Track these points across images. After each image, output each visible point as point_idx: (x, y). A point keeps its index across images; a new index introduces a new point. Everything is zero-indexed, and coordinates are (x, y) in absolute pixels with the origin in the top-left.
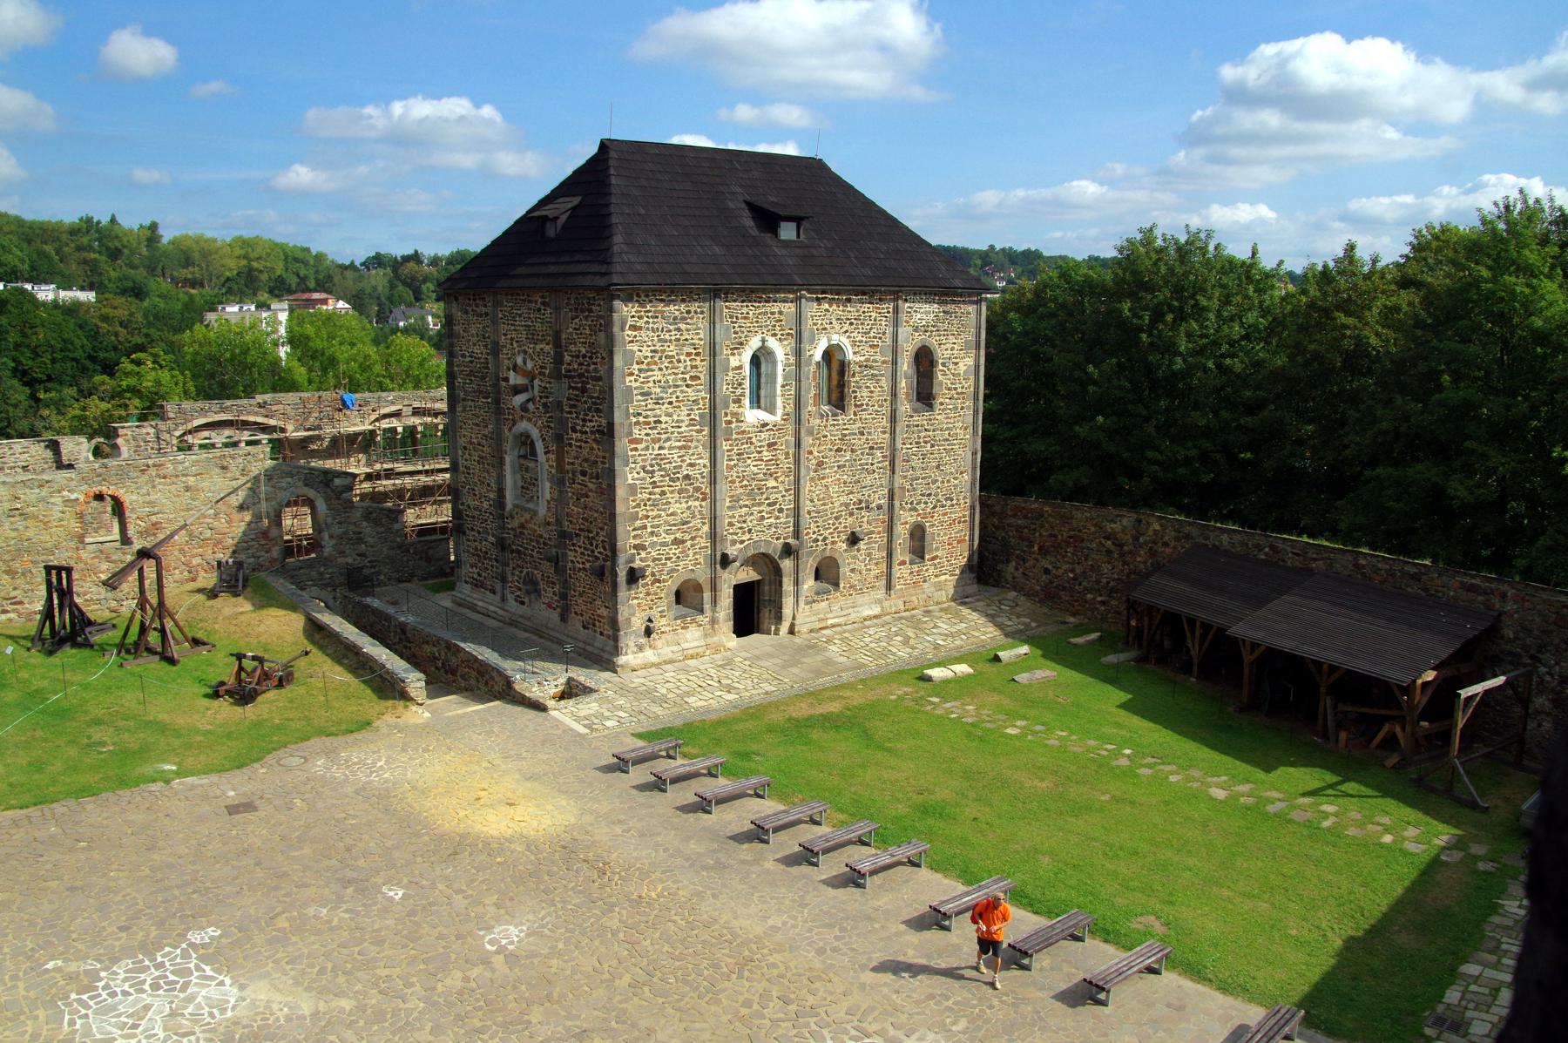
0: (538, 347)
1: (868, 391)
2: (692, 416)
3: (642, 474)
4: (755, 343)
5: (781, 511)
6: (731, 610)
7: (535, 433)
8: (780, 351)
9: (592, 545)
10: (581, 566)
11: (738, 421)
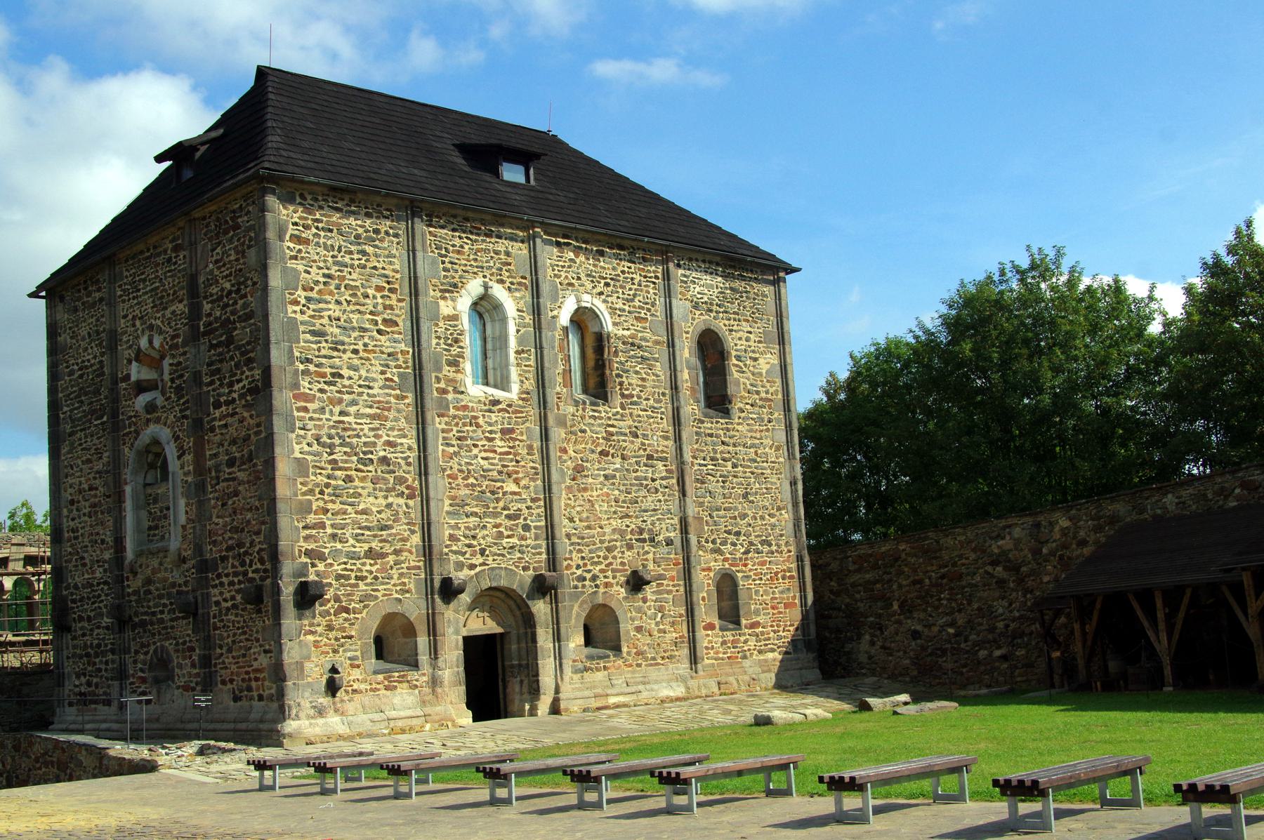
0: (168, 313)
2: (389, 375)
3: (315, 447)
4: (474, 287)
6: (462, 669)
8: (511, 304)
9: (243, 564)
10: (229, 604)
11: (456, 391)
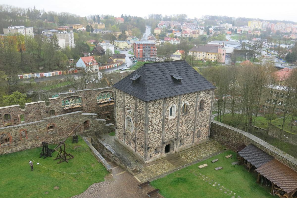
0: (132, 104)
1: (191, 110)
3: (151, 131)
4: (171, 106)
5: (174, 133)
7: (131, 118)
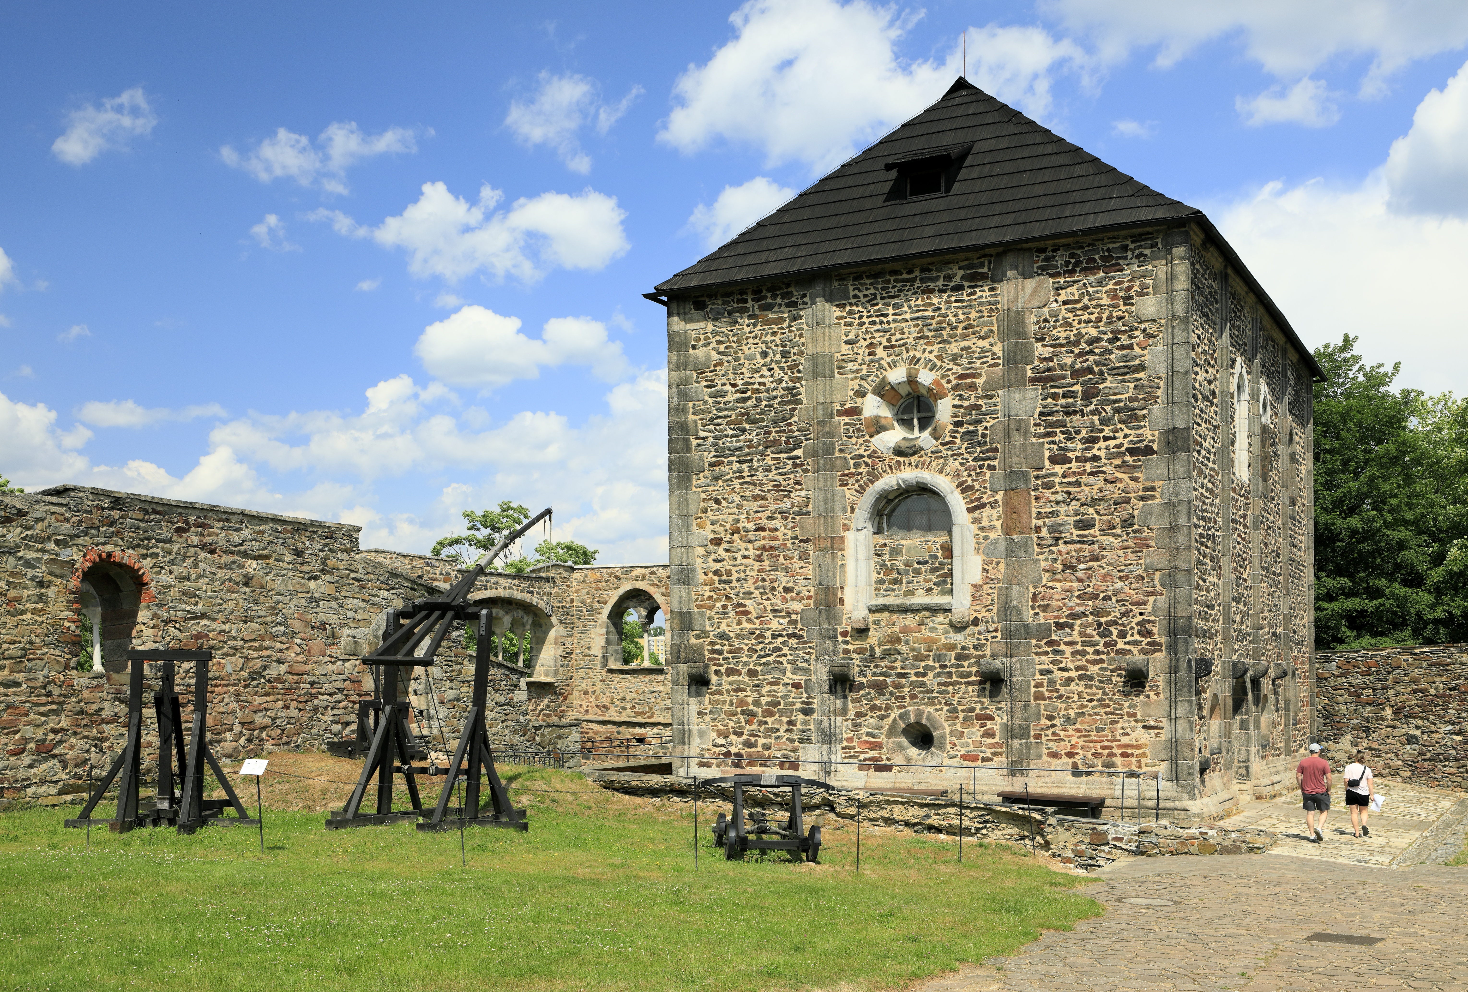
10: (1073, 674)
